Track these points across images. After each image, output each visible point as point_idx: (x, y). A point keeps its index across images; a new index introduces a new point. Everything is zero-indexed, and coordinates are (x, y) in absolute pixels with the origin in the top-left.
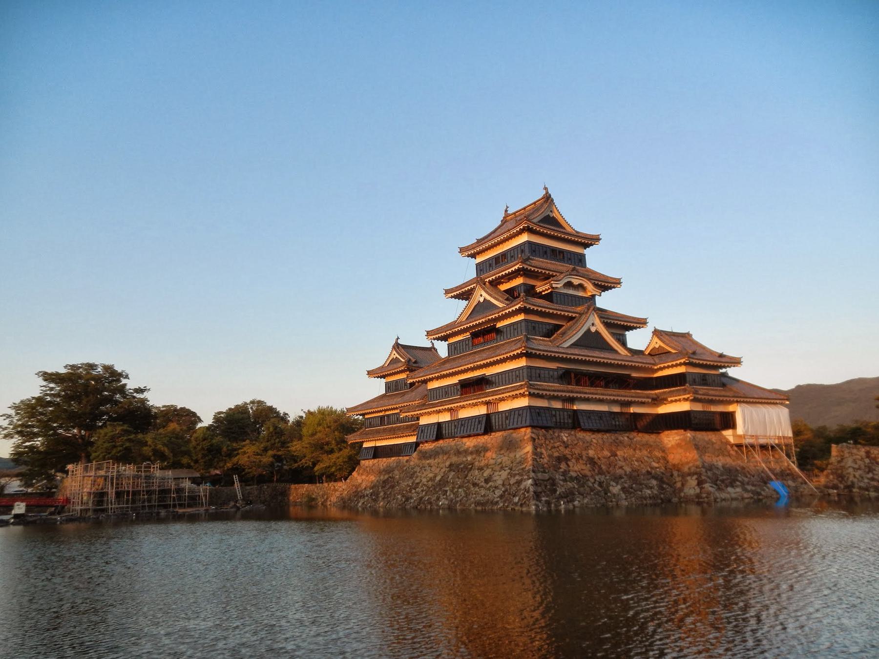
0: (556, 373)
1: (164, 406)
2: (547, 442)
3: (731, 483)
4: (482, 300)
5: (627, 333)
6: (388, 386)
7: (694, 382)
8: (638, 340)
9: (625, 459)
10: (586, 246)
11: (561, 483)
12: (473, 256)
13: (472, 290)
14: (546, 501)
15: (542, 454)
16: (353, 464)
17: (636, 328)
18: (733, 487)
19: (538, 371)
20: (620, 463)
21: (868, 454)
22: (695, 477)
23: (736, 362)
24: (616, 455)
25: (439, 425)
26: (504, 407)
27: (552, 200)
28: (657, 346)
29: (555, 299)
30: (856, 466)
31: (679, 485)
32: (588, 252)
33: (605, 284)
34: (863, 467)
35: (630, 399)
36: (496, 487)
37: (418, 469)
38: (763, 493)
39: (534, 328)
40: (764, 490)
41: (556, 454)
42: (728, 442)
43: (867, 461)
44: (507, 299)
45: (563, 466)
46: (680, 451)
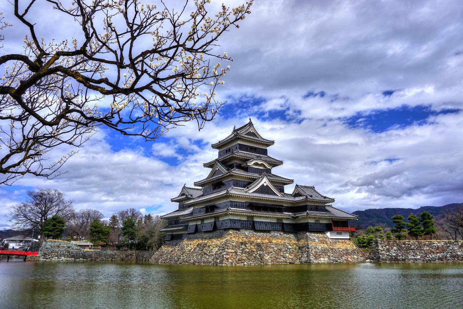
0: (245, 204)
2: (237, 235)
4: (217, 169)
6: (180, 207)
7: (311, 210)
8: (289, 189)
9: (276, 244)
10: (268, 145)
11: (240, 254)
12: (217, 148)
19: (236, 203)
20: (273, 246)
25: (197, 225)
29: (249, 170)
30: (383, 249)
31: (300, 256)
32: (269, 148)
33: (276, 163)
37: (186, 246)
38: (339, 261)
39: (237, 183)
41: (241, 241)
42: (327, 237)
43: (387, 247)
44: (227, 170)
45: (243, 246)
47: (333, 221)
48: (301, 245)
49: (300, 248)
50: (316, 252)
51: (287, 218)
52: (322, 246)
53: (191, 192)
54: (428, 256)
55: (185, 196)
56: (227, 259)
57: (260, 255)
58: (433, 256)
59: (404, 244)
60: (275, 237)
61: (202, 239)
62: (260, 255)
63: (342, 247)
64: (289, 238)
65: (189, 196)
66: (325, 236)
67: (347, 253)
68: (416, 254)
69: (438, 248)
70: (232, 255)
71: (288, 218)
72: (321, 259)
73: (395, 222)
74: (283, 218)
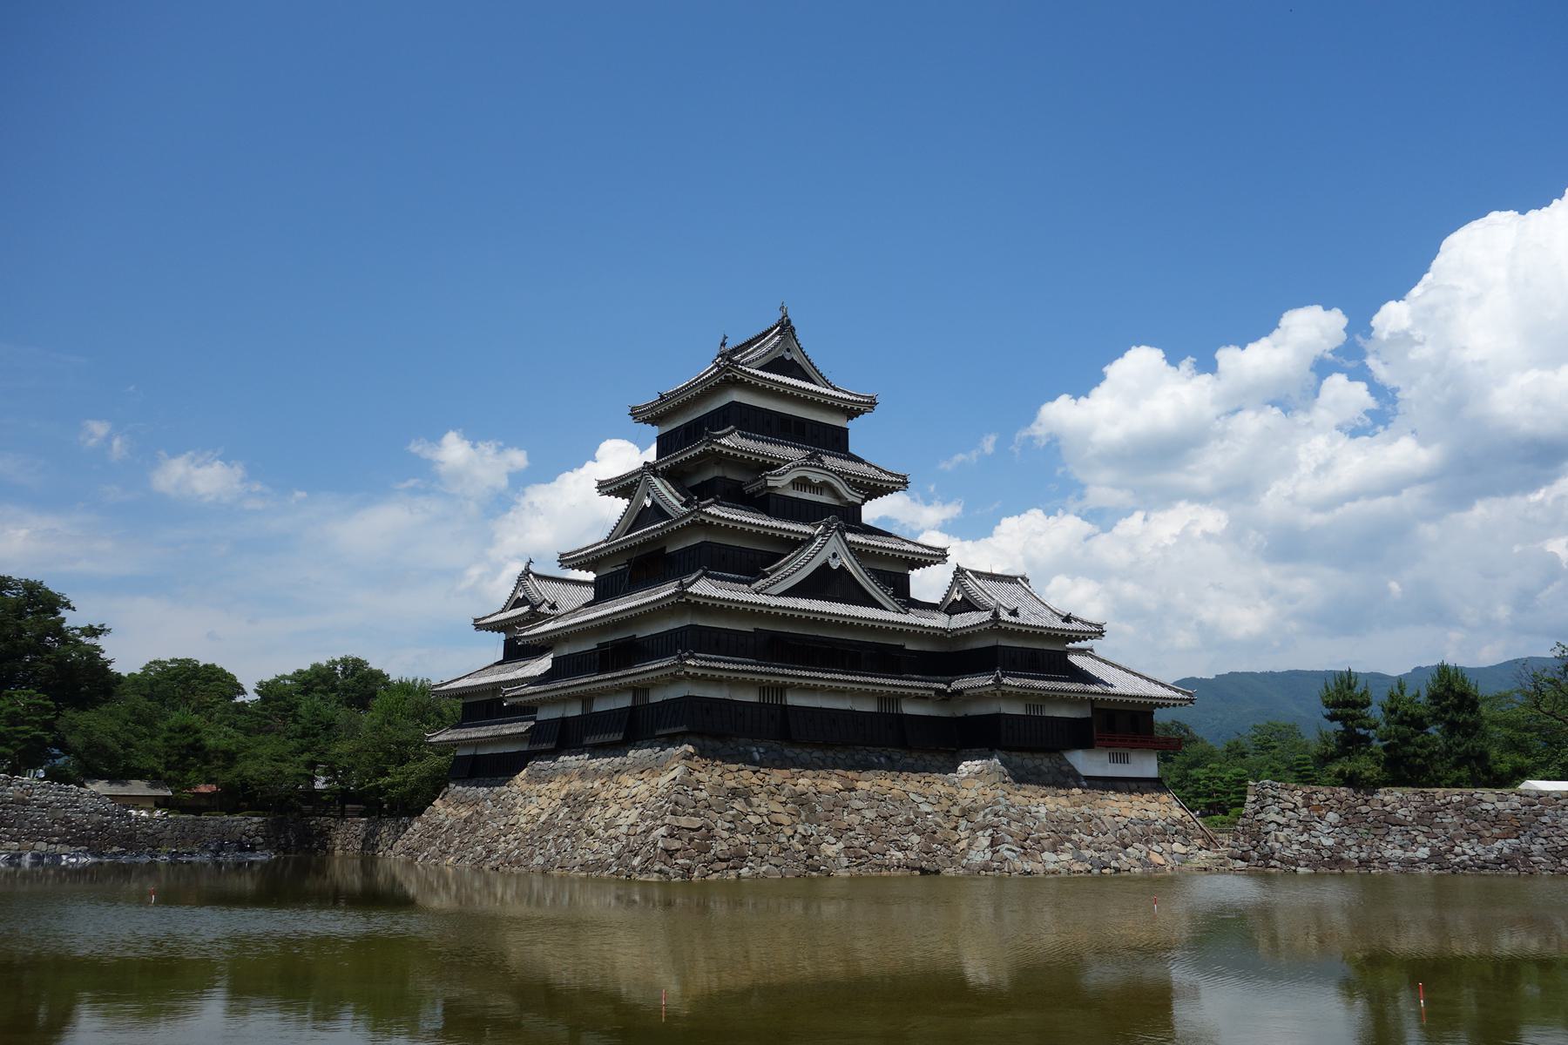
1: (173, 661)
3: (1054, 844)
4: (648, 503)
8: (928, 584)
10: (851, 413)
11: (725, 834)
12: (655, 420)
13: (634, 485)
14: (682, 867)
15: (699, 782)
16: (435, 786)
18: (1055, 851)
20: (859, 804)
21: (1307, 798)
22: (990, 831)
23: (1099, 632)
25: (564, 720)
26: (656, 697)
27: (792, 330)
28: (959, 598)
30: (1282, 820)
34: (1294, 823)
35: (892, 690)
36: (616, 838)
37: (520, 800)
40: (1117, 859)
41: (733, 784)
43: (1304, 811)
45: (739, 805)
46: (979, 784)
47: (1094, 710)
49: (965, 813)
51: (917, 697)
52: (1052, 807)
53: (549, 592)
54: (1457, 849)
55: (526, 608)
56: (670, 853)
57: (805, 839)
58: (1479, 849)
60: (866, 766)
61: (583, 775)
62: (805, 839)
63: (1125, 812)
65: (544, 609)
66: (1065, 768)
67: (1149, 833)
68: (1414, 841)
69: (1497, 818)
70: (691, 839)
71: (924, 698)
72: (1046, 855)
73: (1332, 718)
74: (903, 696)
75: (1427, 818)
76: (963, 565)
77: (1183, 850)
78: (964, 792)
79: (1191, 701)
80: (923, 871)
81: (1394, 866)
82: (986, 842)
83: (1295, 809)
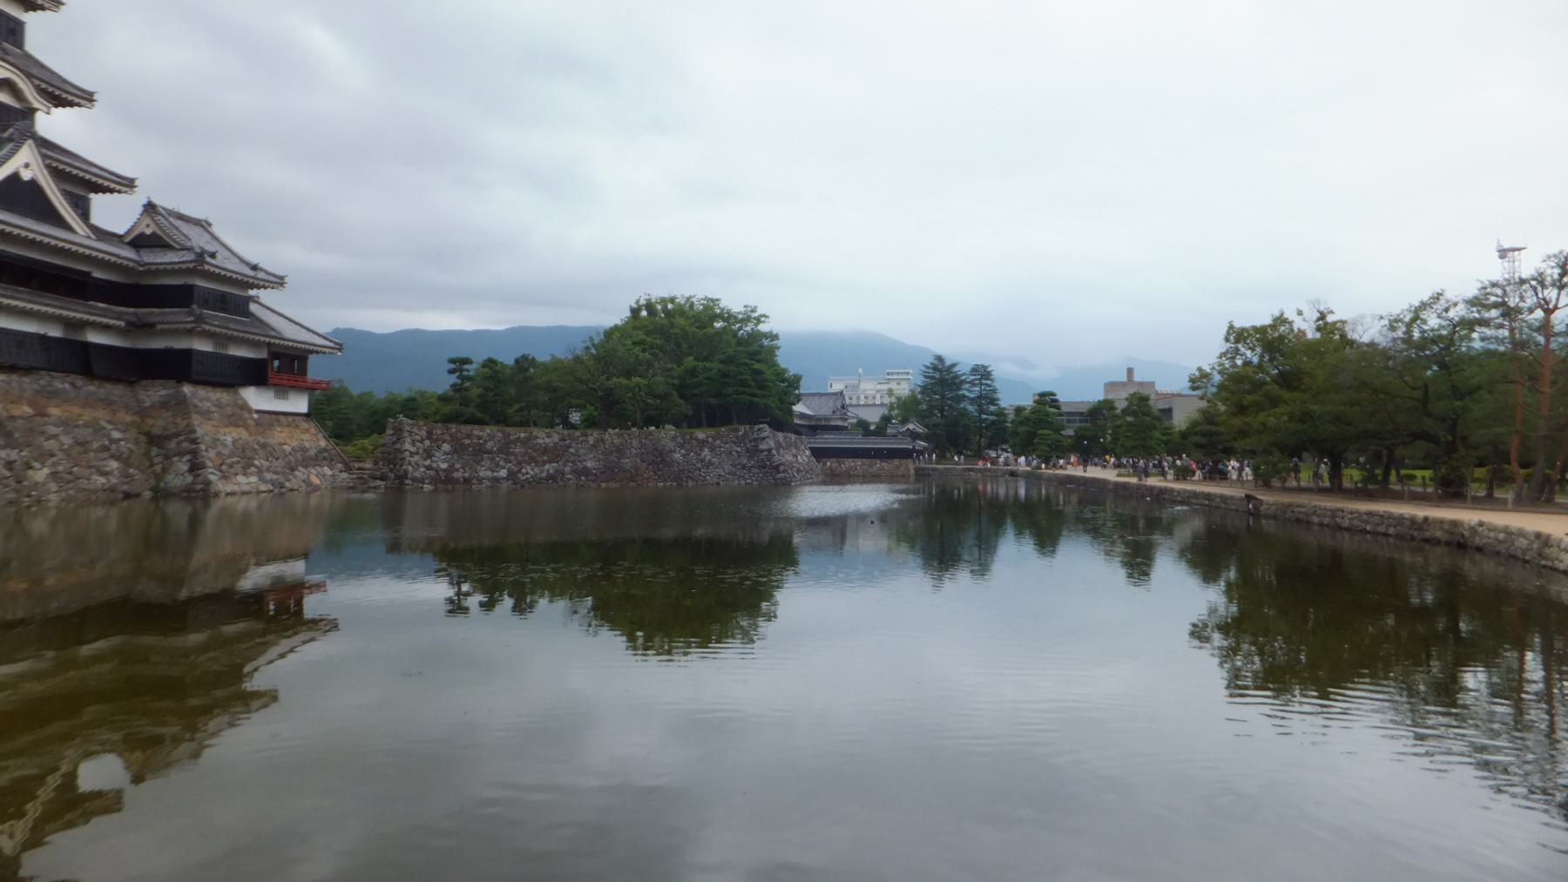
5: (92, 196)
7: (206, 304)
9: (67, 424)
17: (112, 191)
20: (52, 430)
24: (43, 415)
30: (413, 449)
31: (158, 468)
33: (61, 94)
35: (86, 317)
42: (245, 407)
43: (427, 443)
47: (270, 353)
48: (156, 431)
49: (153, 440)
50: (219, 454)
52: (235, 435)
59: (468, 436)
60: (54, 395)
64: (108, 403)
73: (451, 372)
75: (505, 449)
76: (156, 201)
77: (330, 472)
78: (150, 421)
79: (340, 350)
80: (127, 496)
81: (486, 483)
82: (185, 468)
83: (422, 441)
